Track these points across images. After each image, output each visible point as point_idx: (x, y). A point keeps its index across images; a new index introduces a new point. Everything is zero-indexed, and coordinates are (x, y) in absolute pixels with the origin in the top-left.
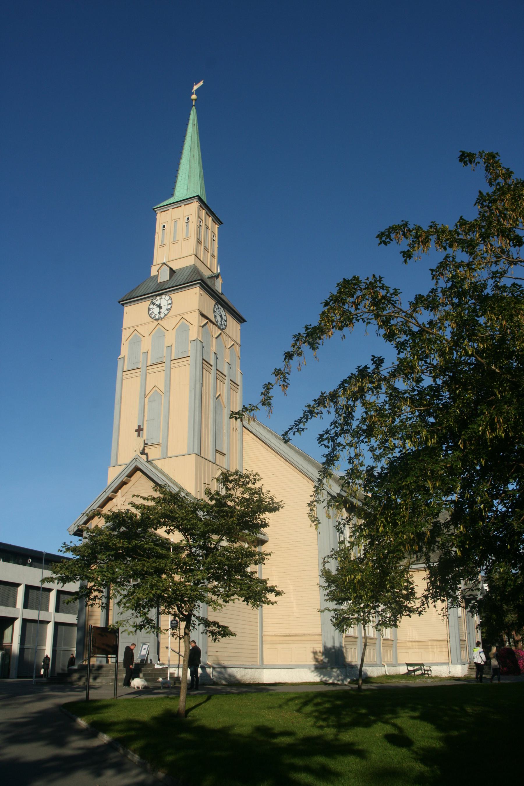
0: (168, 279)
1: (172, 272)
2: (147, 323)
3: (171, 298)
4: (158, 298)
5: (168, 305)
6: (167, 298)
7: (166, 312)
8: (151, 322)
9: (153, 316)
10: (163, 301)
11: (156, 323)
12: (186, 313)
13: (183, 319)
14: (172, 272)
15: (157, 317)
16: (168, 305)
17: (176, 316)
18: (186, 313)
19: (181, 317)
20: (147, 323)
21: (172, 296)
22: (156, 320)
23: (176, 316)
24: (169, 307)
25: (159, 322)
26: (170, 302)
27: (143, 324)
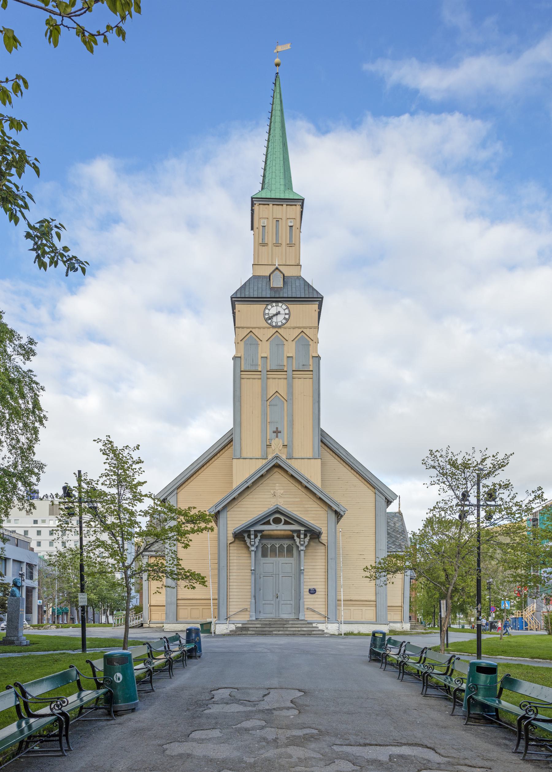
0: (282, 286)
2: (264, 328)
4: (274, 304)
5: (286, 314)
6: (284, 307)
7: (284, 321)
8: (268, 328)
11: (275, 330)
13: (303, 334)
16: (286, 314)
17: (294, 328)
20: (264, 328)
21: (289, 306)
22: (273, 327)
23: (294, 328)
24: (287, 316)
26: (287, 311)
27: (259, 328)
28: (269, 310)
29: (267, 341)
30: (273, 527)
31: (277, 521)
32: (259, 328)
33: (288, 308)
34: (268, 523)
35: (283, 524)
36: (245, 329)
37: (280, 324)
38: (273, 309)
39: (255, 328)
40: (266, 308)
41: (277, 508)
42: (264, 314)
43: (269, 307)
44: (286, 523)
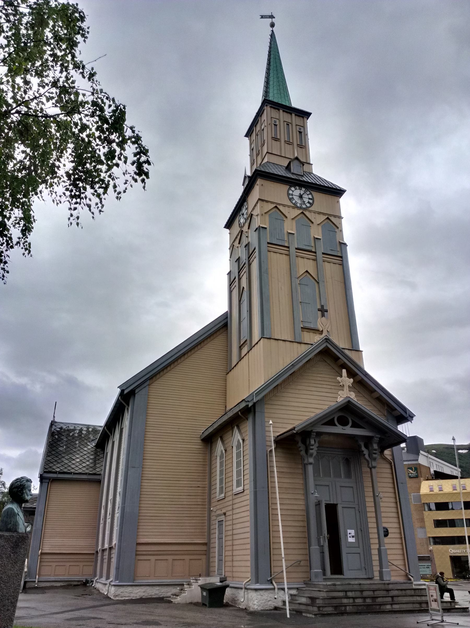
2: (289, 207)
4: (298, 188)
8: (293, 208)
9: (294, 202)
20: (289, 207)
24: (311, 201)
27: (284, 205)
28: (293, 191)
29: (293, 219)
30: (339, 429)
31: (343, 422)
32: (284, 205)
33: (311, 194)
34: (331, 423)
35: (351, 427)
36: (269, 204)
38: (296, 192)
39: (280, 204)
41: (349, 402)
42: (288, 194)
43: (293, 189)
44: (355, 425)
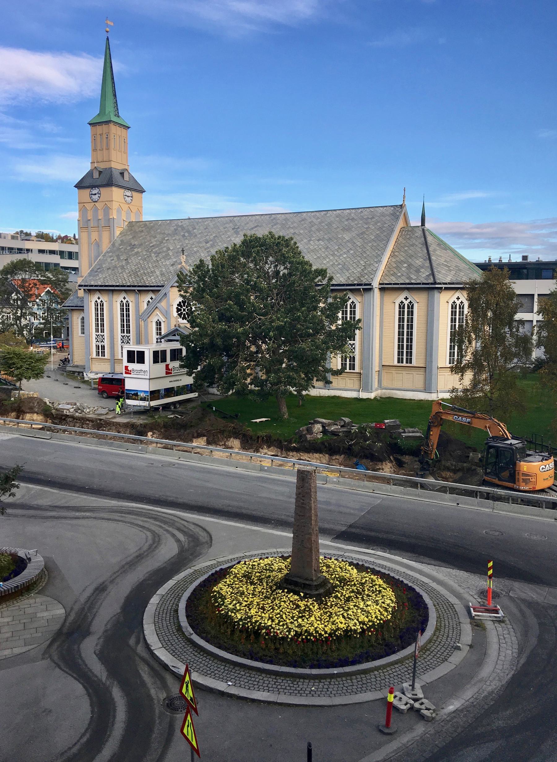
1: (100, 172)
3: (100, 191)
6: (98, 190)
7: (98, 198)
10: (95, 191)
11: (94, 203)
12: (108, 201)
14: (100, 172)
15: (94, 200)
17: (103, 202)
18: (108, 201)
19: (105, 203)
23: (103, 202)
25: (95, 203)
37: (96, 200)
40: (90, 191)
43: (92, 190)
